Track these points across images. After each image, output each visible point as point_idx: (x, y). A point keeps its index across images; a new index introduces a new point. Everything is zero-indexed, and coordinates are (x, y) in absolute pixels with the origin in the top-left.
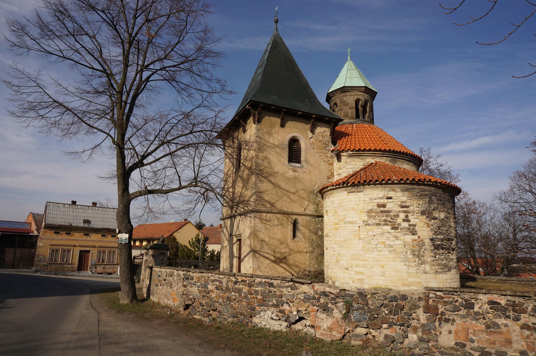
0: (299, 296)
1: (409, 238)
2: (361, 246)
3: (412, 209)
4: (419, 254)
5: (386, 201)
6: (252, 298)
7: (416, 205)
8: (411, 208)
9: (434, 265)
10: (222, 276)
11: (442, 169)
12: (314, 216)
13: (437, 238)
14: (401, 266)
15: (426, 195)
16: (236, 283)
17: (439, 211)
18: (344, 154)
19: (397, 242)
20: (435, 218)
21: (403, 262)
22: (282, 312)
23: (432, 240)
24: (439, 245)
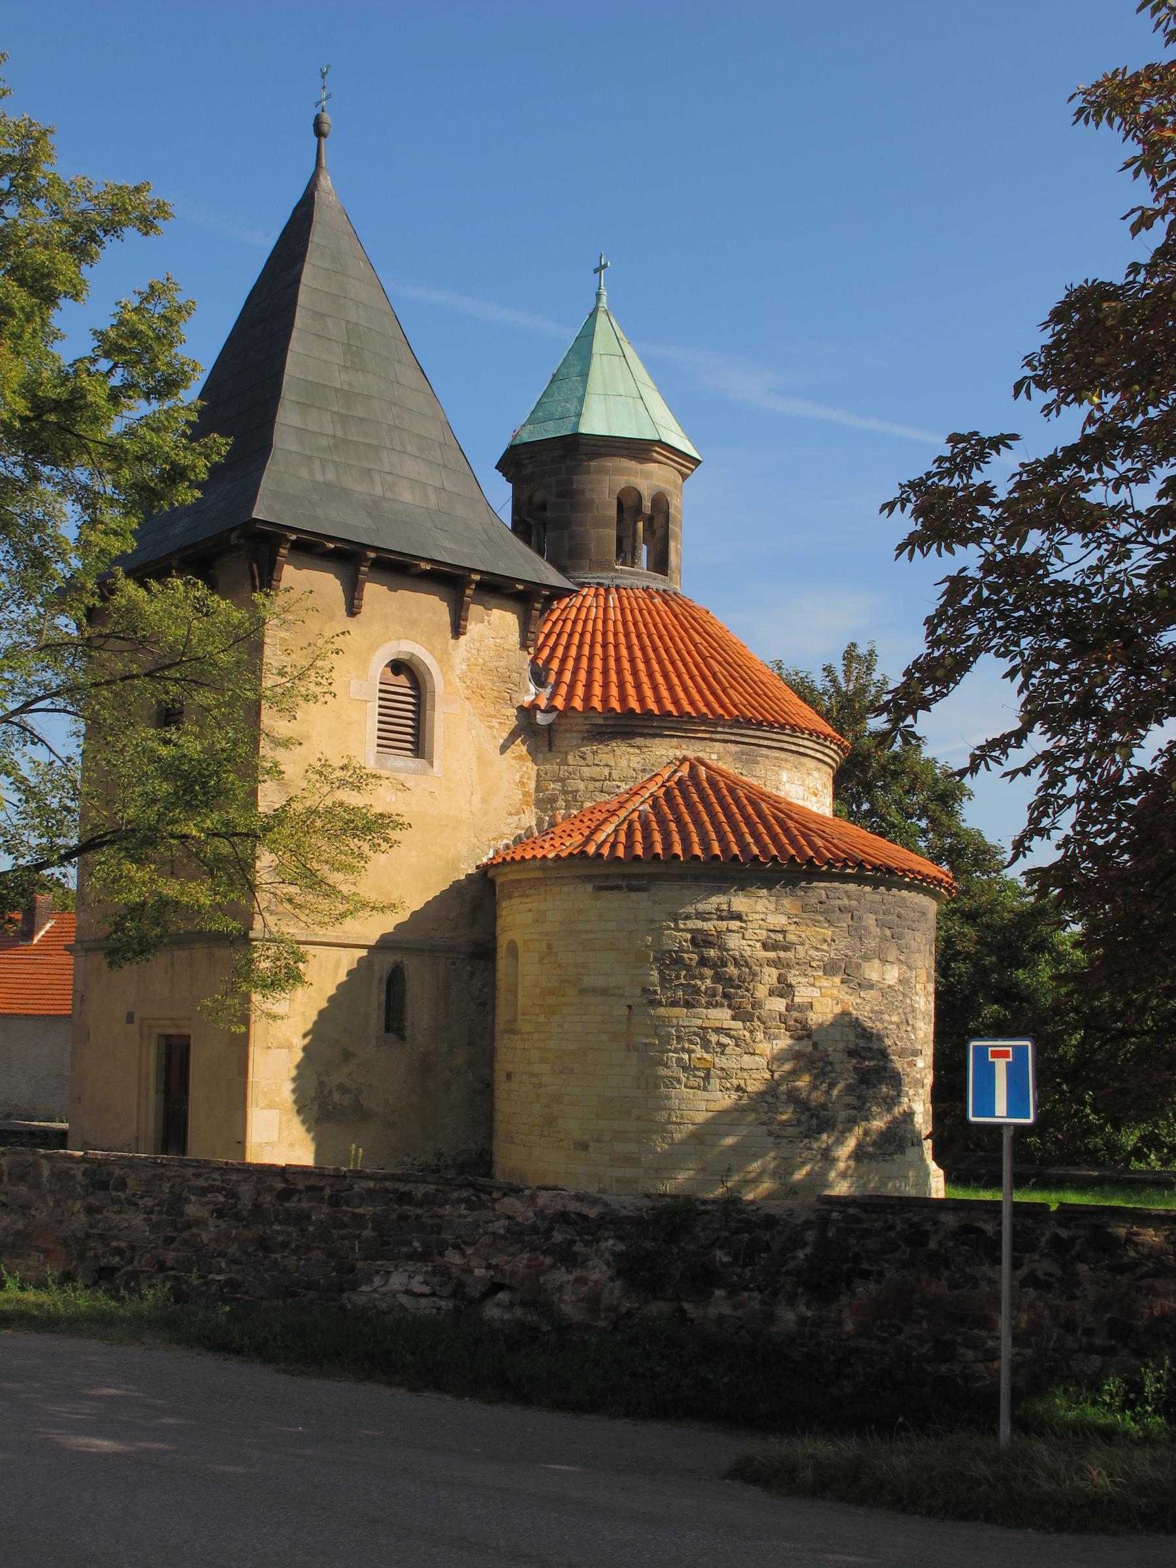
0: (491, 1228)
6: (343, 1237)
21: (764, 1124)
22: (443, 1272)
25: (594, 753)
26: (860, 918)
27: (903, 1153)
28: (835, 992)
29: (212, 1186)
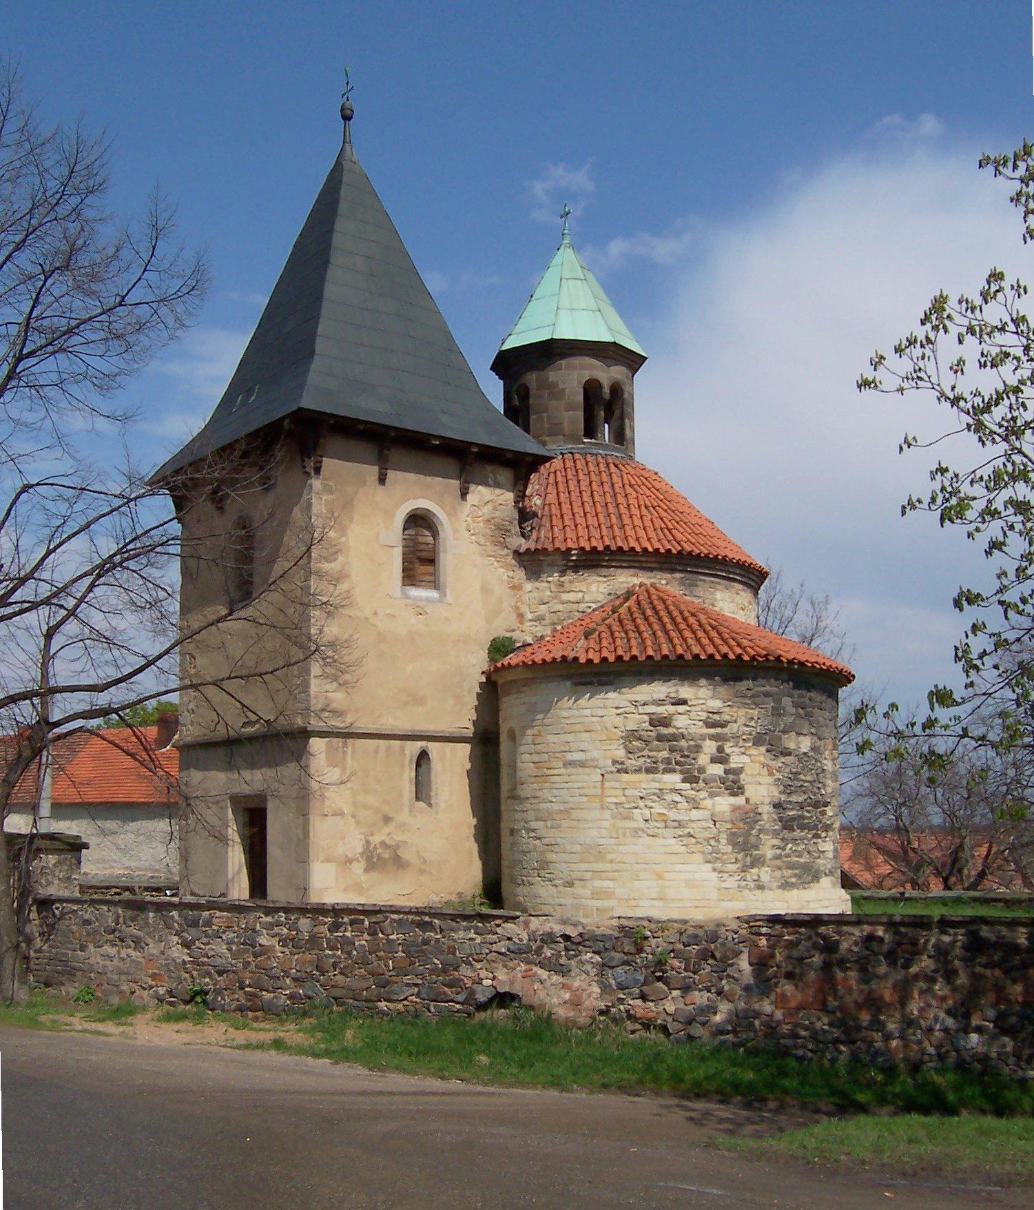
1: (724, 803)
2: (606, 824)
3: (735, 731)
4: (746, 842)
5: (671, 709)
8: (732, 728)
9: (779, 868)
14: (705, 872)
15: (767, 695)
17: (799, 734)
19: (695, 814)
20: (786, 753)
21: (709, 862)
23: (777, 806)
24: (793, 819)
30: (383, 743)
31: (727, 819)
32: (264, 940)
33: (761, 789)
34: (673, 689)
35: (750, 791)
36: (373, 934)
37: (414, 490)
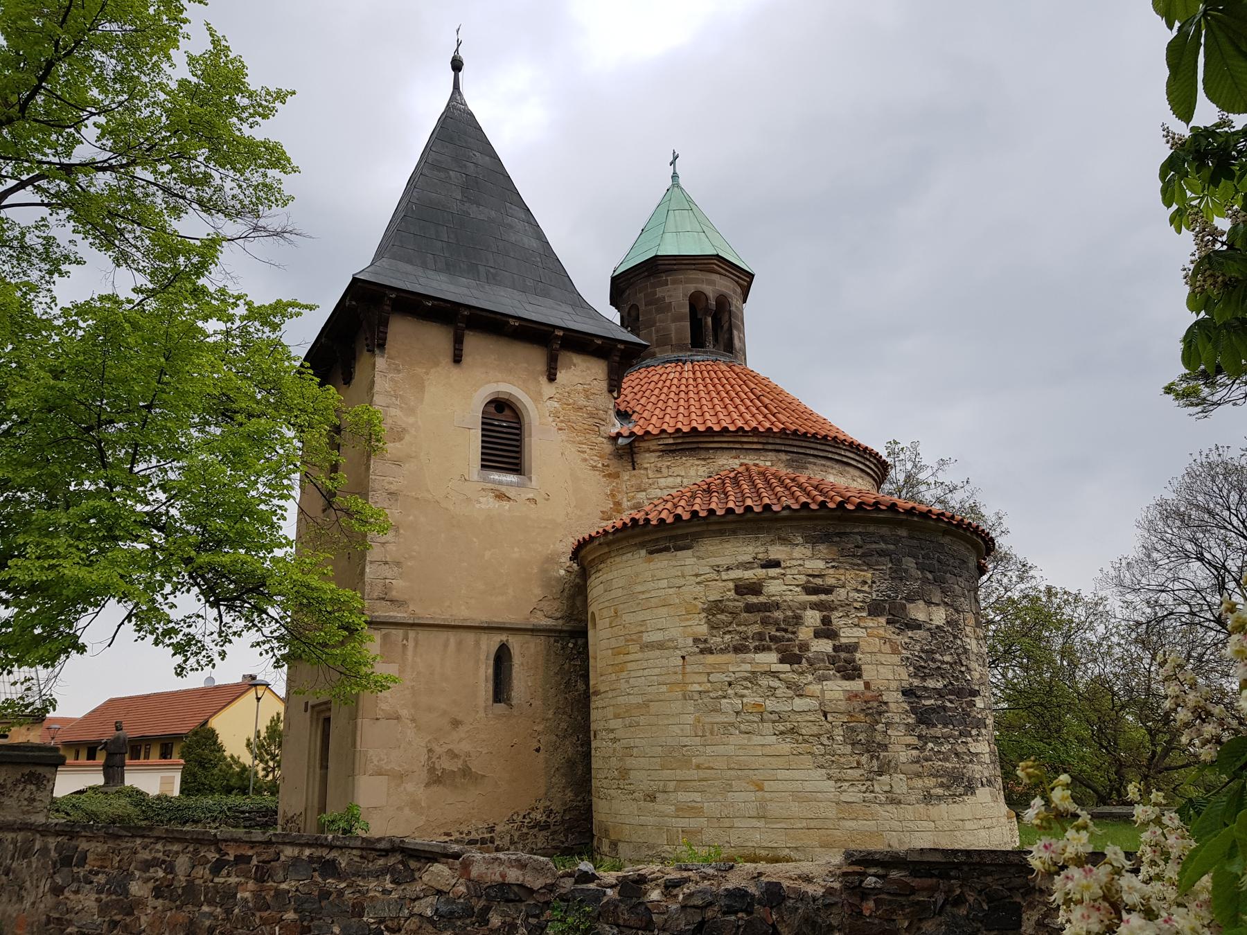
0: (419, 907)
1: (836, 689)
2: (690, 719)
3: (843, 597)
5: (761, 572)
6: (264, 922)
7: (853, 584)
8: (841, 594)
9: (919, 775)
10: (175, 848)
11: (955, 500)
12: (561, 631)
13: (926, 689)
14: (817, 781)
15: (882, 553)
16: (217, 868)
18: (653, 445)
19: (799, 704)
21: (822, 767)
23: (908, 693)
24: (933, 709)
25: (668, 467)
26: (900, 561)
27: (973, 793)
28: (881, 631)
29: (154, 858)
30: (452, 637)
31: (842, 709)
32: (137, 888)
33: (885, 669)
34: (762, 549)
35: (868, 673)
36: (260, 880)
37: (495, 373)
